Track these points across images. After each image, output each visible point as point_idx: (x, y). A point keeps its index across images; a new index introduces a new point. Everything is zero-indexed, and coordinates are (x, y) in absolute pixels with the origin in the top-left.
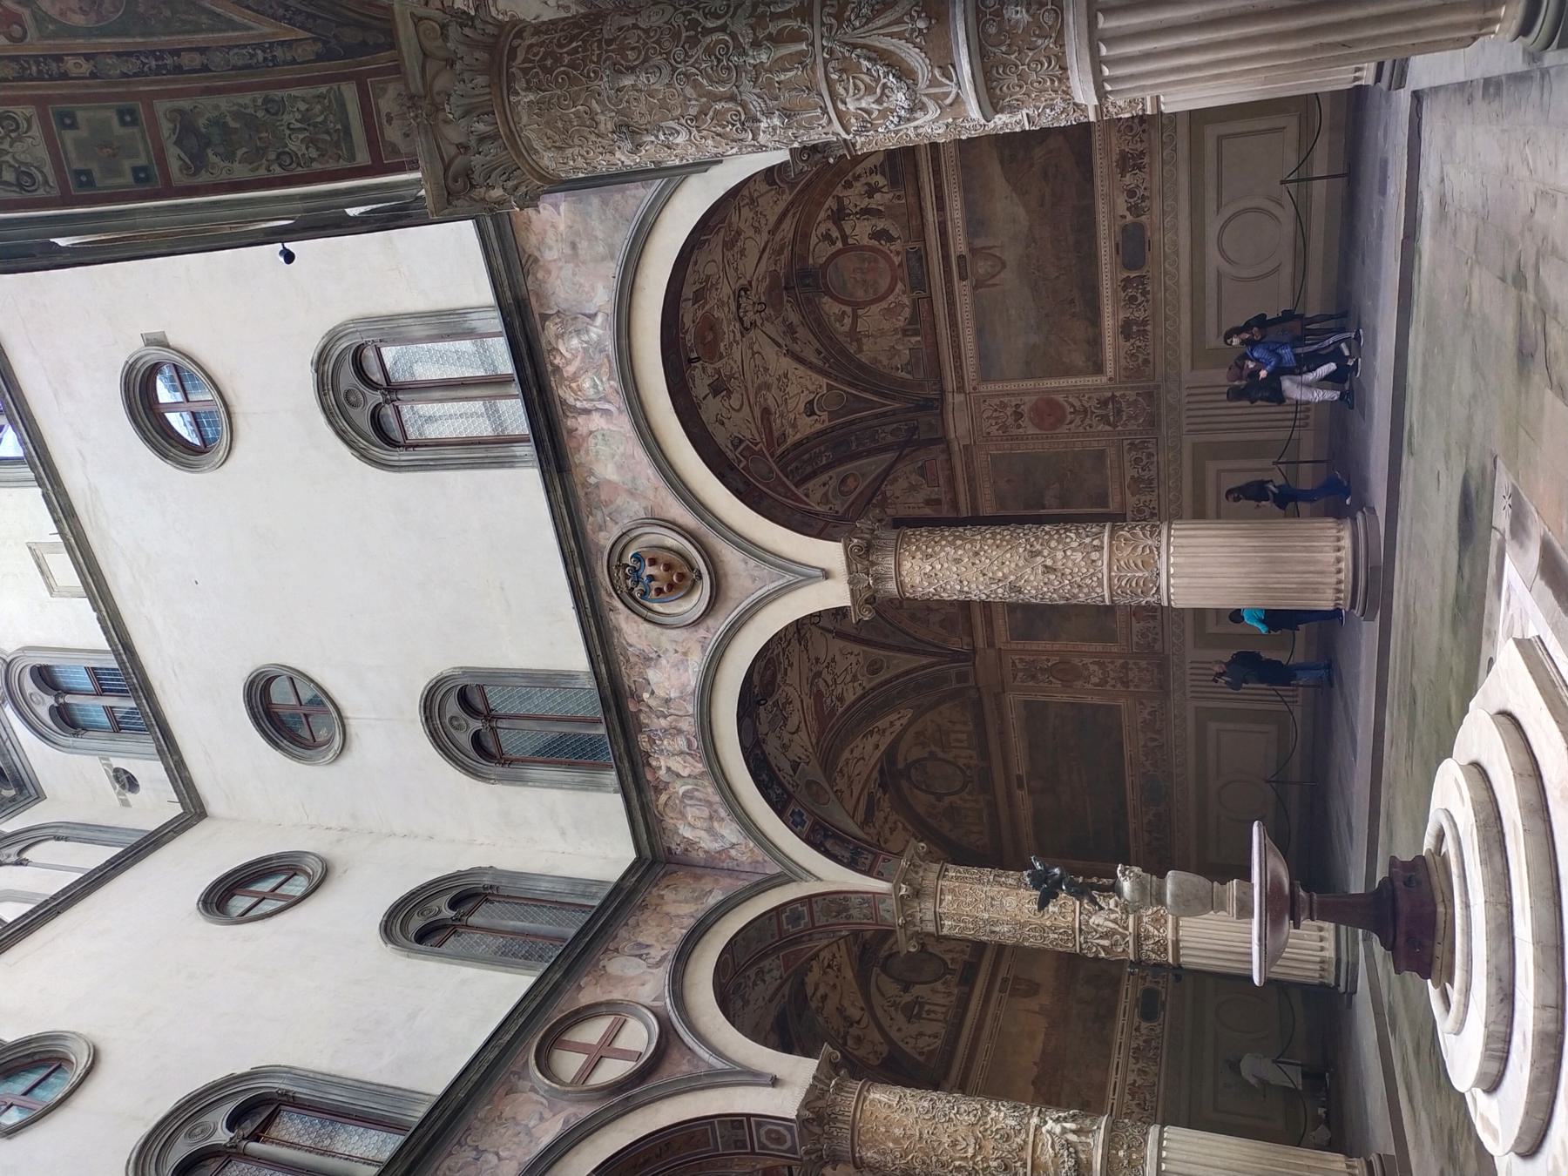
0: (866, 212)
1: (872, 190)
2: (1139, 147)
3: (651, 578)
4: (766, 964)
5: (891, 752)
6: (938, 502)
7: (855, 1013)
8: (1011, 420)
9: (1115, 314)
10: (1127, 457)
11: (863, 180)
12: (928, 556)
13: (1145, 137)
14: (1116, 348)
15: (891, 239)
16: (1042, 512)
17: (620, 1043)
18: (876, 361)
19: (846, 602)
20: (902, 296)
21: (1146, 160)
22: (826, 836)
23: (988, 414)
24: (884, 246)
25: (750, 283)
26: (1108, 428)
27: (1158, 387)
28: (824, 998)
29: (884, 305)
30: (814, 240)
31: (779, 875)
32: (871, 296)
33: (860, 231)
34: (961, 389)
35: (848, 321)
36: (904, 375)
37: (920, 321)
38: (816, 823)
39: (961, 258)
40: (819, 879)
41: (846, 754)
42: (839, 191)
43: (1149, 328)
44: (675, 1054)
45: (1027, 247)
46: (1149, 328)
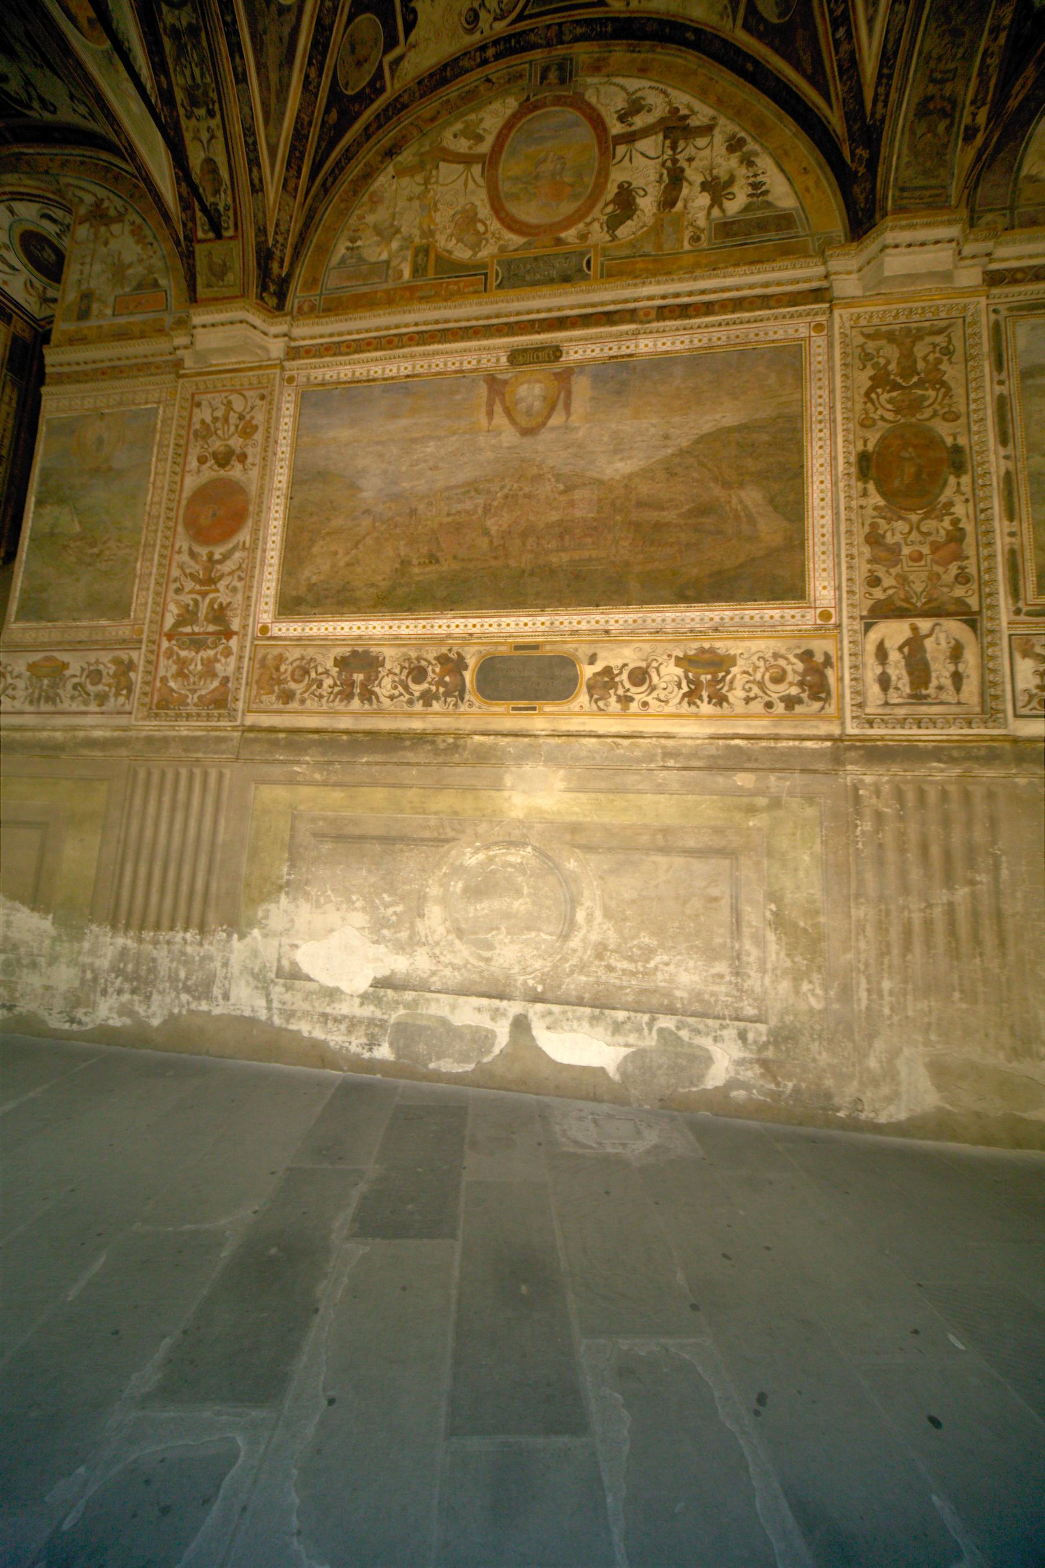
0: (676, 178)
1: (717, 188)
2: (736, 695)
6: (84, 314)
8: (216, 445)
9: (396, 640)
10: (106, 657)
11: (742, 171)
13: (757, 707)
14: (325, 643)
15: (613, 224)
16: (31, 501)
18: (375, 202)
20: (498, 241)
21: (706, 708)
23: (238, 404)
24: (601, 212)
26: (169, 621)
27: (232, 717)
29: (484, 211)
30: (633, 84)
32: (505, 187)
33: (641, 168)
34: (294, 353)
35: (463, 145)
36: (341, 249)
37: (438, 274)
39: (555, 352)
42: (726, 127)
43: (356, 704)
45: (558, 477)
46: (356, 704)
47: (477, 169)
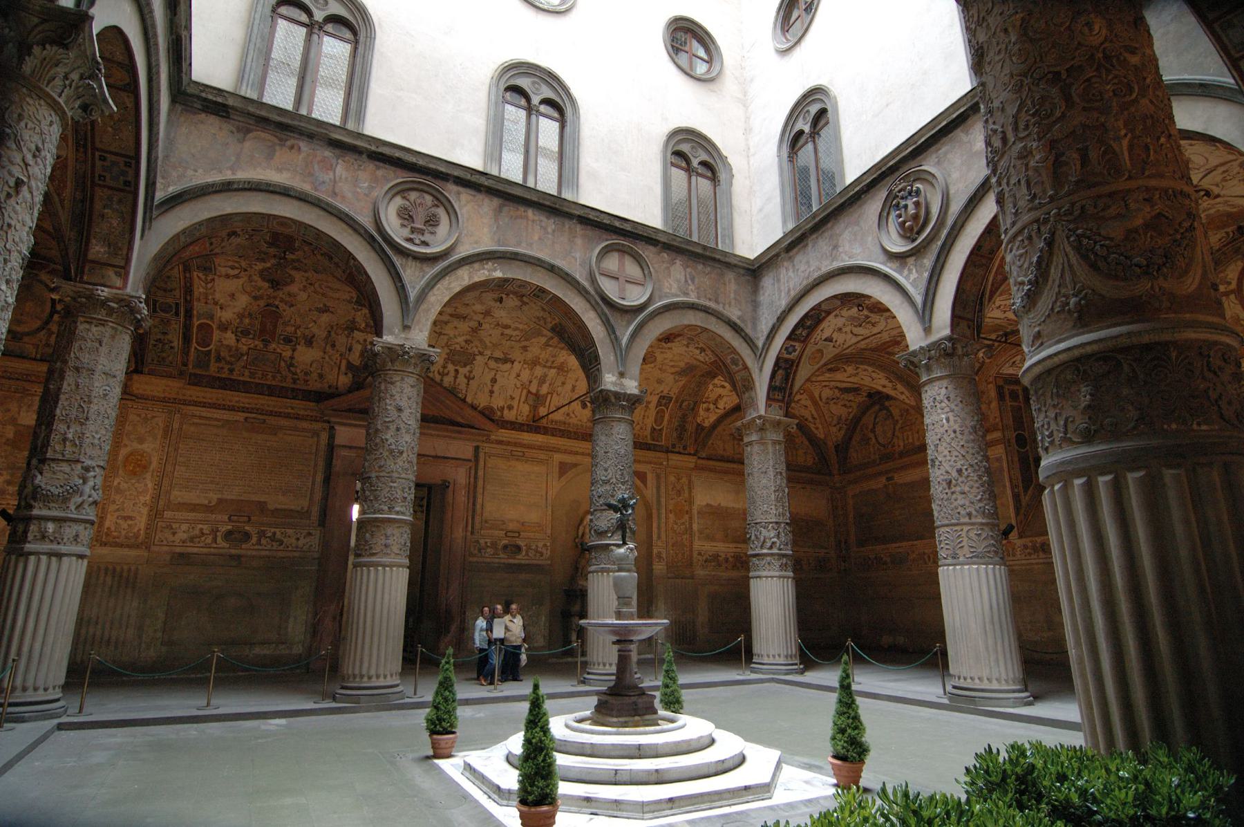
3: (906, 207)
4: (709, 352)
5: (888, 397)
7: (721, 405)
12: (948, 398)
17: (629, 286)
19: (912, 348)
22: (786, 369)
25: (1218, 196)
28: (723, 387)
31: (756, 347)
38: (793, 361)
40: (761, 370)
41: (870, 369)
44: (627, 317)
47: (1232, 297)
